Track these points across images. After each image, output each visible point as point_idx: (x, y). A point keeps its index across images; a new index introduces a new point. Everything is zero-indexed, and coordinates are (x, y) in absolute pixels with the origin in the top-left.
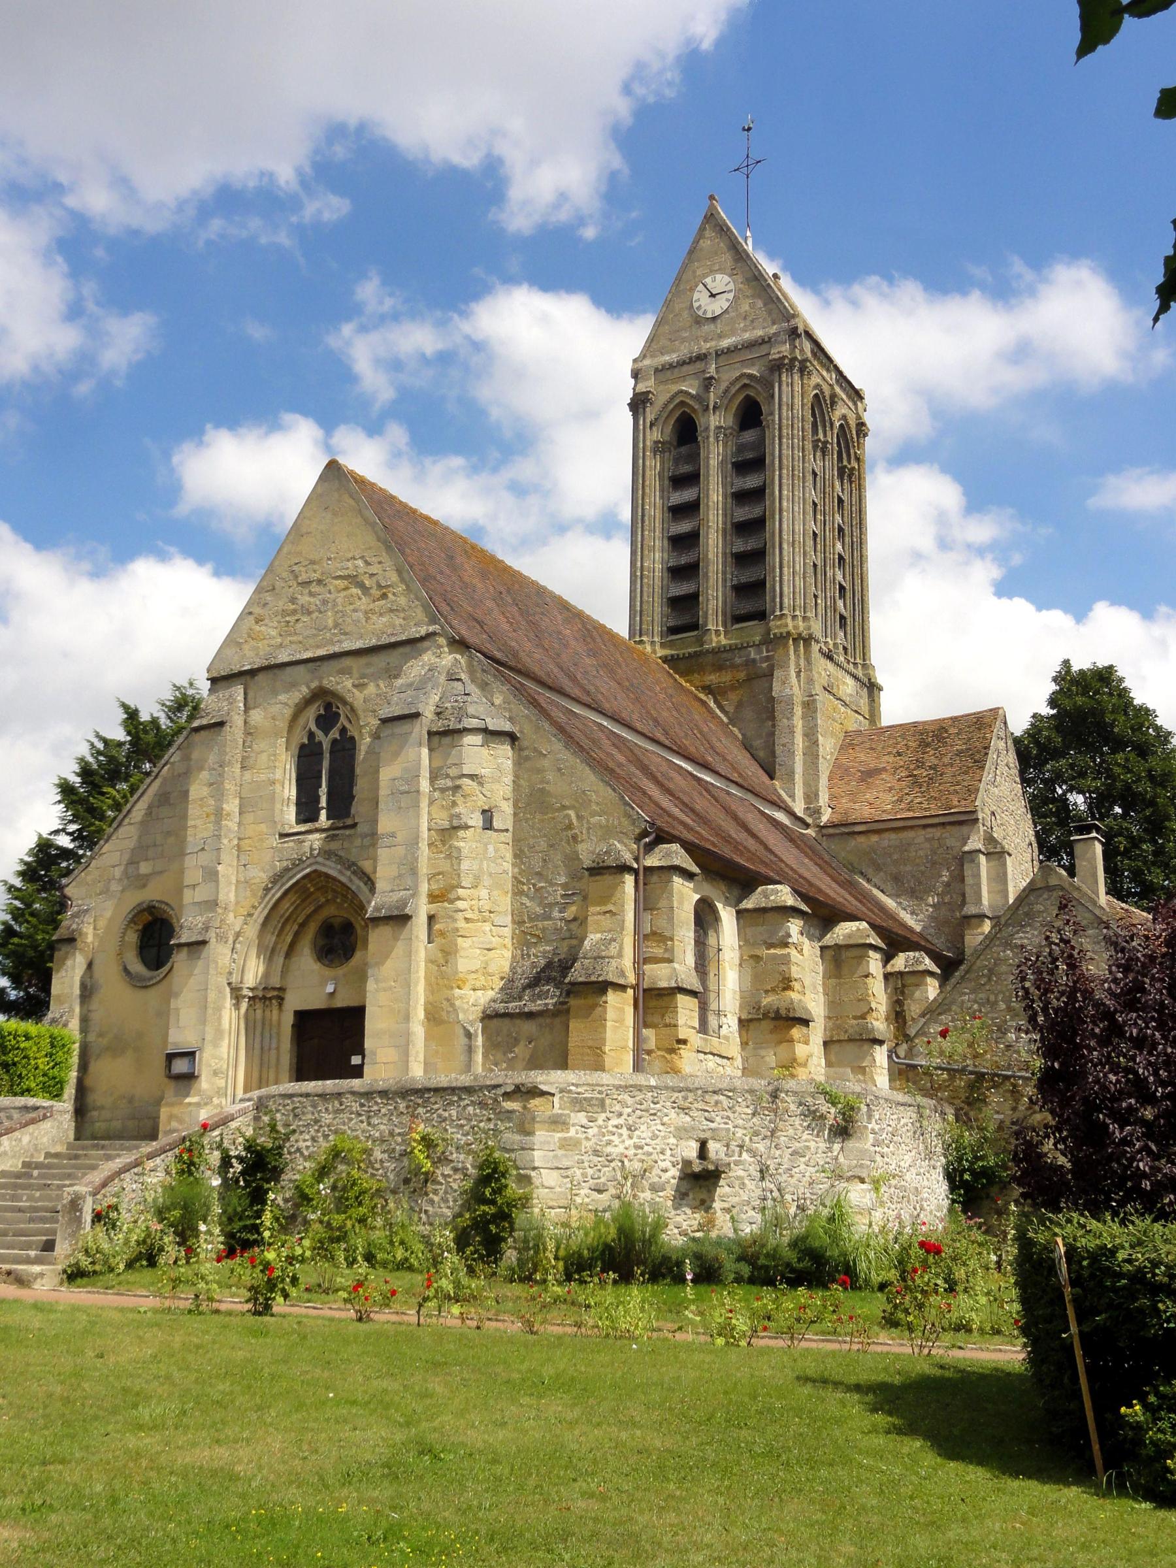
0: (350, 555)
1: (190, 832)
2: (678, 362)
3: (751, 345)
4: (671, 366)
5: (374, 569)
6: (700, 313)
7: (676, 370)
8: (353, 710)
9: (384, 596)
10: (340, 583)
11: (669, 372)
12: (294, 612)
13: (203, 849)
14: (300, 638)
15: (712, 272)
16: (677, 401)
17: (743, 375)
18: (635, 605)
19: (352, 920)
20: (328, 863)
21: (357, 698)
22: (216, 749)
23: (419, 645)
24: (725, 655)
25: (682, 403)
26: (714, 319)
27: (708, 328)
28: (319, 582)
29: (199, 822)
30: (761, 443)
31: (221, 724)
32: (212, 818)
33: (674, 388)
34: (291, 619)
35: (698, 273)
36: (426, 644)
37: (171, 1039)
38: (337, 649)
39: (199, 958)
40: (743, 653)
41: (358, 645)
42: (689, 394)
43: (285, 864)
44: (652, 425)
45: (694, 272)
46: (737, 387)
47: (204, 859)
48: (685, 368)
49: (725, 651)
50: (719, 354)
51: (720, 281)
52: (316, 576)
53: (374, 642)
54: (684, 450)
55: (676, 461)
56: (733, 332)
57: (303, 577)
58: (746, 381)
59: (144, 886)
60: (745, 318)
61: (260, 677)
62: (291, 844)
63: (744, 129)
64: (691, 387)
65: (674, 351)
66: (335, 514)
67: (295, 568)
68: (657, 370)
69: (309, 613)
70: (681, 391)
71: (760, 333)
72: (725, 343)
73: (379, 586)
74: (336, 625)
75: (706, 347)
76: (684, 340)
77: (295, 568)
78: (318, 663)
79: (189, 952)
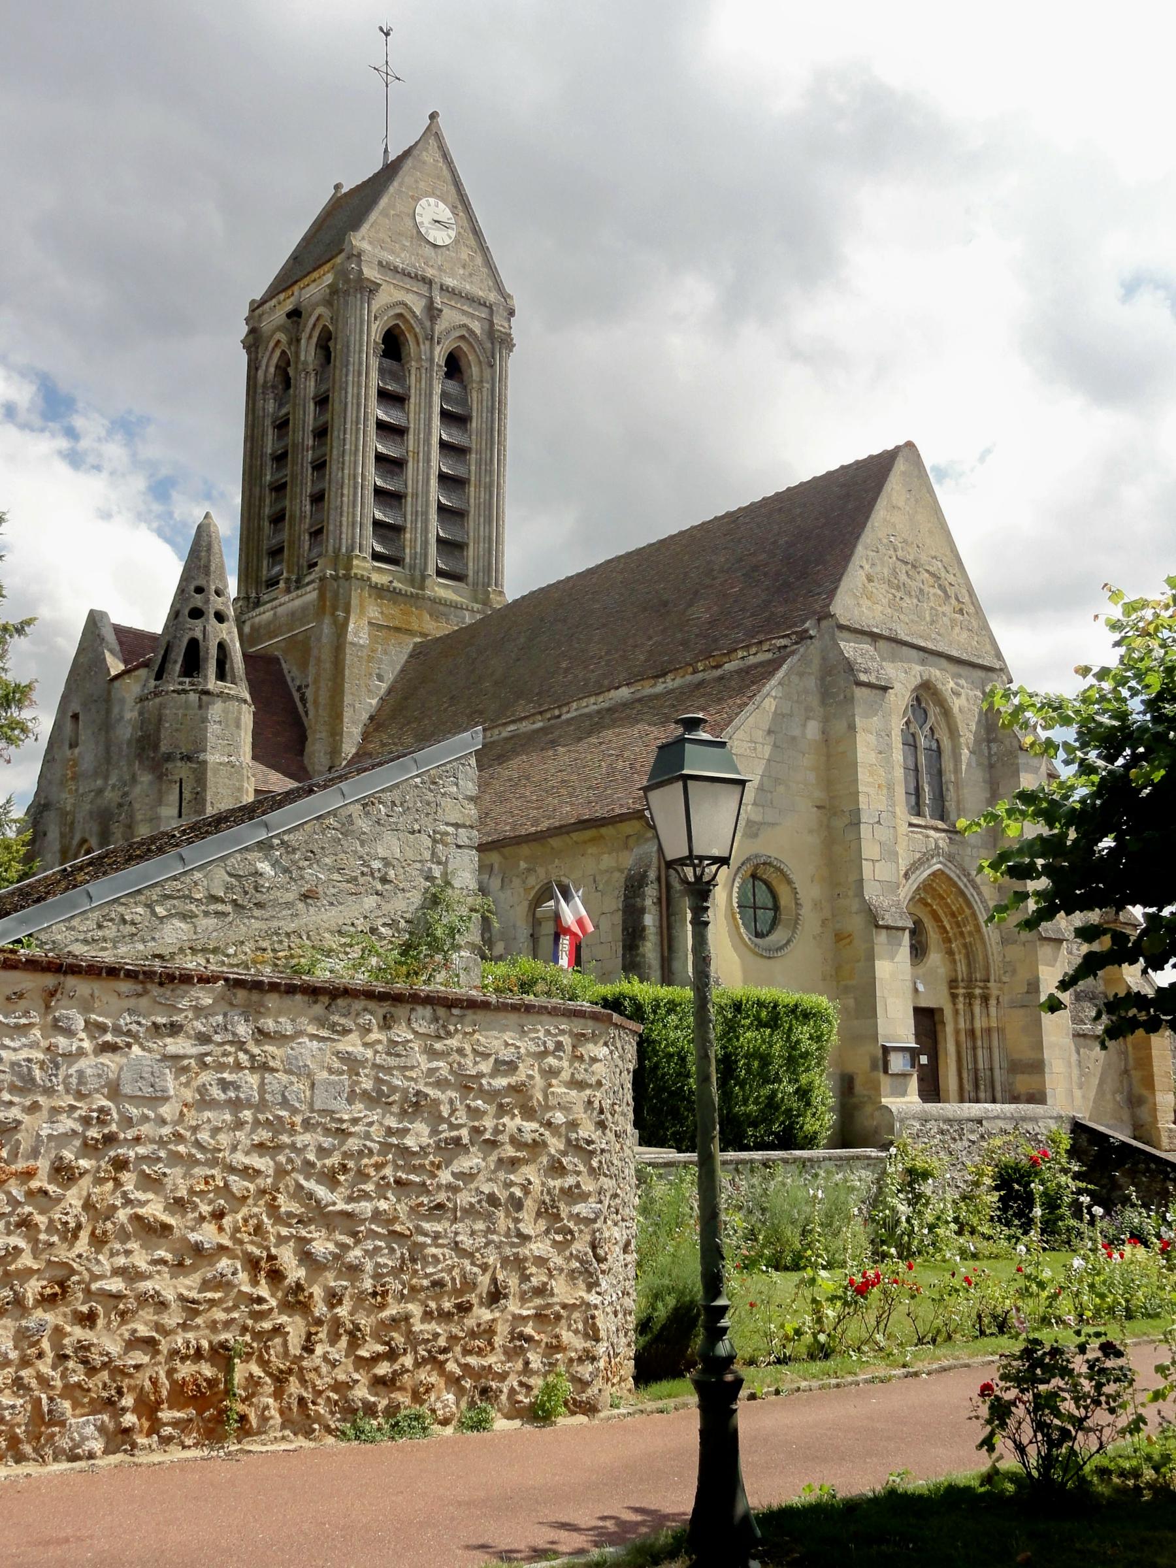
0: (933, 554)
1: (862, 798)
2: (403, 270)
3: (471, 299)
4: (395, 270)
5: (951, 578)
6: (423, 231)
7: (398, 276)
8: (946, 712)
9: (961, 611)
10: (931, 580)
11: (390, 273)
12: (898, 588)
13: (879, 822)
14: (907, 620)
15: (433, 195)
16: (398, 311)
17: (465, 326)
18: (354, 515)
19: (925, 920)
20: (949, 864)
21: (956, 704)
22: (880, 713)
23: (990, 674)
24: (441, 608)
25: (400, 316)
26: (435, 246)
27: (428, 250)
28: (914, 566)
29: (871, 791)
30: (464, 401)
31: (885, 689)
32: (885, 791)
33: (399, 296)
34: (899, 595)
35: (422, 185)
36: (994, 676)
37: (881, 1031)
38: (941, 647)
39: (900, 945)
40: (459, 612)
41: (955, 653)
42: (414, 313)
43: (918, 855)
44: (376, 318)
45: (416, 181)
46: (458, 334)
47: (882, 833)
48: (407, 280)
49: (446, 605)
50: (443, 288)
51: (444, 212)
52: (910, 558)
53: (965, 657)
54: (388, 363)
55: (382, 371)
56: (453, 276)
57: (900, 553)
58: (465, 333)
59: (756, 835)
60: (464, 267)
61: (881, 644)
62: (920, 836)
63: (381, 29)
64: (418, 307)
65: (393, 252)
66: (917, 501)
67: (892, 539)
68: (380, 263)
69: (911, 596)
70: (406, 305)
71: (481, 293)
72: (450, 282)
73: (957, 599)
74: (933, 622)
75: (430, 273)
76: (404, 248)
77: (892, 539)
78: (926, 655)
79: (888, 936)
